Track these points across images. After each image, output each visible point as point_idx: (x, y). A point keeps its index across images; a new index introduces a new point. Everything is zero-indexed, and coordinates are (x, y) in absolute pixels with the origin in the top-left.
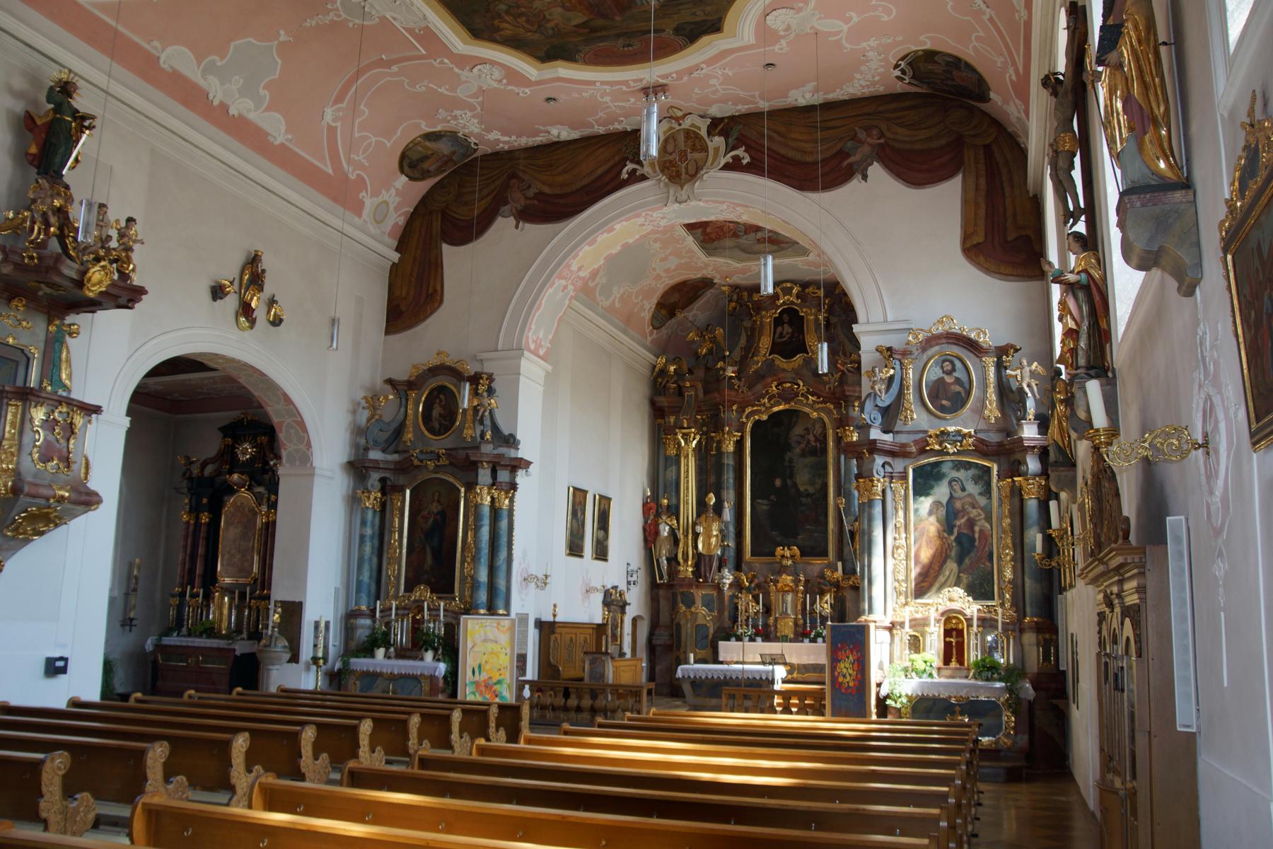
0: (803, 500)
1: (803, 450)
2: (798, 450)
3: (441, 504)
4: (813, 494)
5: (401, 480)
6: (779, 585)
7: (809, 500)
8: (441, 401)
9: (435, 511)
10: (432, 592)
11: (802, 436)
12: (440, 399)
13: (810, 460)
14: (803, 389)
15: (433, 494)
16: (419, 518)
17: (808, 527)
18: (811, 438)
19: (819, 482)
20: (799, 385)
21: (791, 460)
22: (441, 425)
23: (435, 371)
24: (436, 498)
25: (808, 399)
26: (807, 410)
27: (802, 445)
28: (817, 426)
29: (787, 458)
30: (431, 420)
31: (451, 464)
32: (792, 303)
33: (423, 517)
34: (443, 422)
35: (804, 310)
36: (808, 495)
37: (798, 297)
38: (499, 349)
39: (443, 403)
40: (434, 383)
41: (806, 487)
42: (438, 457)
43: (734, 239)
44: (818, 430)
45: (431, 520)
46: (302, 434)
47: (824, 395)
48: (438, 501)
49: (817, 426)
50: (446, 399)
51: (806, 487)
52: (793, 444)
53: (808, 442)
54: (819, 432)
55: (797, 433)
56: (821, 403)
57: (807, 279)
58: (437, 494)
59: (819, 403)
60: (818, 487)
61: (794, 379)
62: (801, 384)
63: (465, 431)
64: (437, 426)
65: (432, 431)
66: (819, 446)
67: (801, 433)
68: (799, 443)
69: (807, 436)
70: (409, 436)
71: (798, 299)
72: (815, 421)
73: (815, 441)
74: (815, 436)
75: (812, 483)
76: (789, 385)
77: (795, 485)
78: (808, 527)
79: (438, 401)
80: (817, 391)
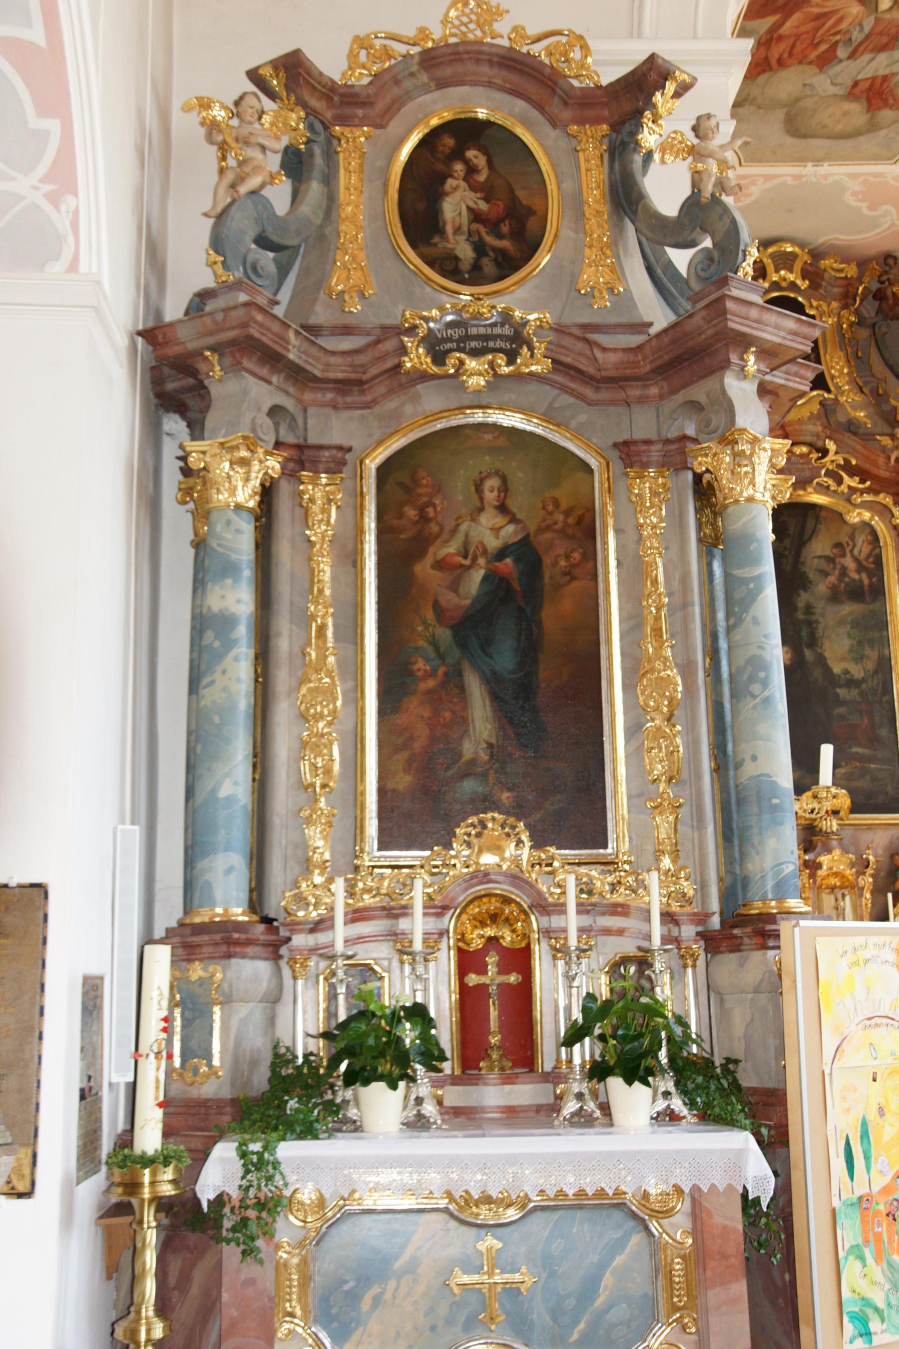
0: (842, 692)
1: (834, 588)
2: (822, 588)
3: (513, 520)
4: (863, 680)
6: (821, 873)
7: (855, 692)
8: (471, 170)
9: (493, 543)
10: (538, 843)
11: (830, 560)
12: (466, 162)
13: (848, 609)
14: (834, 458)
15: (479, 488)
16: (423, 569)
17: (855, 750)
18: (849, 563)
19: (874, 655)
20: (825, 452)
21: (809, 609)
22: (480, 248)
24: (491, 496)
25: (840, 481)
26: (840, 506)
27: (832, 579)
28: (861, 539)
29: (801, 604)
30: (441, 232)
32: (793, 286)
33: (440, 565)
34: (489, 239)
35: (815, 303)
36: (851, 683)
37: (805, 275)
39: (482, 177)
41: (844, 665)
43: (814, 69)
44: (862, 547)
45: (477, 575)
46: (35, 122)
47: (884, 474)
48: (502, 508)
49: (861, 539)
50: (490, 163)
51: (844, 665)
52: (812, 576)
53: (844, 571)
54: (866, 549)
55: (819, 553)
56: (868, 491)
57: (821, 240)
58: (493, 483)
59: (862, 492)
60: (870, 665)
61: (817, 435)
62: (831, 446)
64: (465, 252)
66: (866, 581)
67: (828, 552)
68: (826, 574)
69: (842, 561)
71: (804, 278)
72: (854, 528)
73: (858, 571)
74: (856, 560)
75: (859, 659)
76: (805, 449)
77: (821, 661)
78: (855, 750)
79: (459, 168)
80: (867, 466)
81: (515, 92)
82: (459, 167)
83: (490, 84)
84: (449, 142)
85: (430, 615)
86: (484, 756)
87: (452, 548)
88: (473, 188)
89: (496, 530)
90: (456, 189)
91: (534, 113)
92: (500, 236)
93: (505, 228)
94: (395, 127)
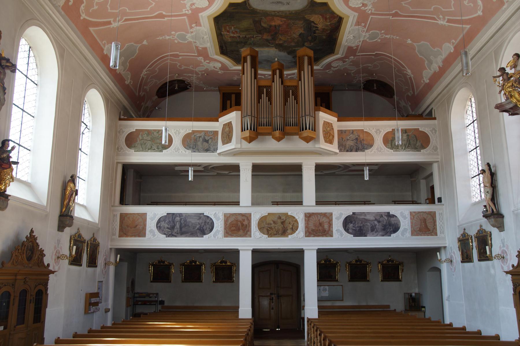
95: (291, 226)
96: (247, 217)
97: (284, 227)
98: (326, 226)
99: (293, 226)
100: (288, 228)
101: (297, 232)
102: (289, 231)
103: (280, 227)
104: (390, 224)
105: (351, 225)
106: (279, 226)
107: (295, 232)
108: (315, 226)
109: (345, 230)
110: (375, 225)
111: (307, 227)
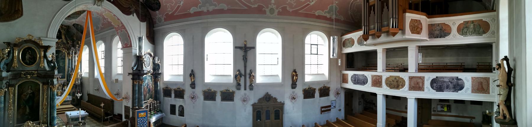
3: (32, 90)
5: (13, 82)
8: (29, 53)
9: (30, 92)
15: (29, 87)
16: (22, 96)
22: (30, 61)
23: (26, 41)
24: (30, 88)
31: (37, 76)
33: (24, 95)
34: (31, 60)
38: (48, 37)
39: (30, 54)
40: (26, 46)
42: (33, 74)
45: (28, 96)
48: (31, 89)
50: (31, 52)
58: (30, 86)
63: (41, 64)
64: (28, 62)
65: (26, 63)
70: (16, 64)
81: (34, 45)
82: (28, 52)
83: (32, 44)
84: (27, 50)
85: (23, 100)
86: (28, 114)
87: (26, 93)
88: (29, 55)
89: (30, 91)
90: (27, 55)
91: (36, 47)
92: (32, 60)
93: (33, 59)
94: (21, 47)
95: (401, 84)
96: (380, 77)
97: (398, 84)
98: (421, 85)
99: (402, 83)
100: (400, 85)
101: (404, 87)
102: (400, 87)
103: (396, 84)
104: (458, 85)
105: (435, 85)
106: (395, 83)
107: (403, 87)
108: (415, 84)
109: (431, 87)
110: (449, 85)
111: (410, 85)
